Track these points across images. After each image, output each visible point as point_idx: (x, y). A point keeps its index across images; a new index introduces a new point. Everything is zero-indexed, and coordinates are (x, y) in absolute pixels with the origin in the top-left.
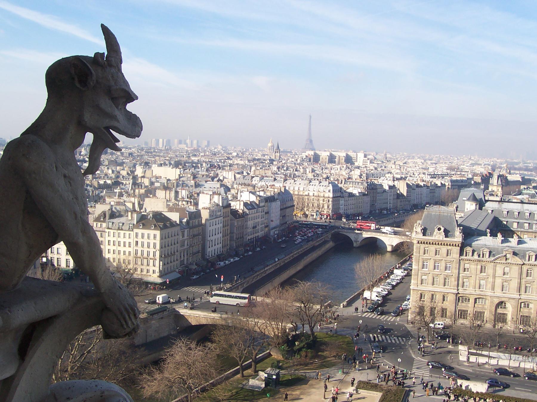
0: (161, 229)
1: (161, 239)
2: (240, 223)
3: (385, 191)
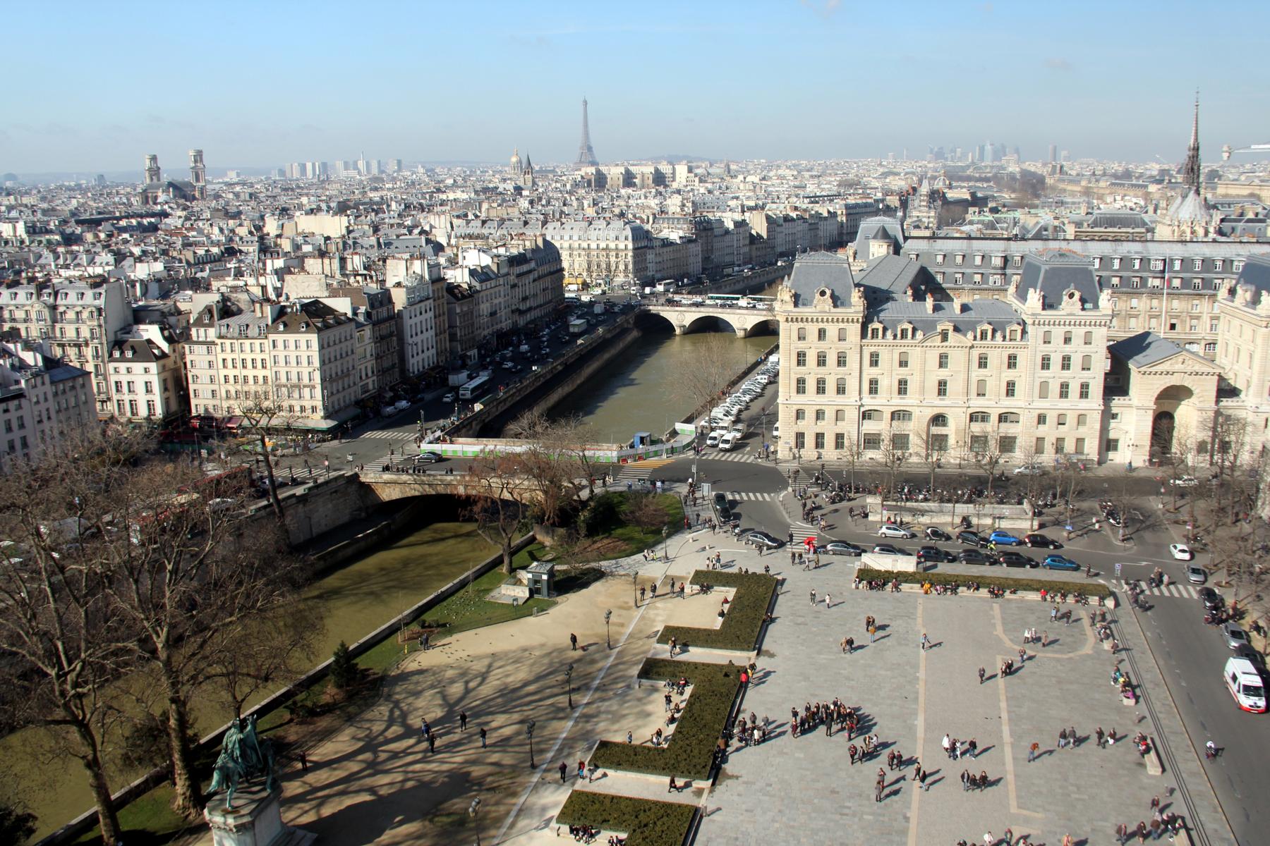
0: (319, 330)
1: (322, 347)
2: (465, 309)
3: (727, 232)
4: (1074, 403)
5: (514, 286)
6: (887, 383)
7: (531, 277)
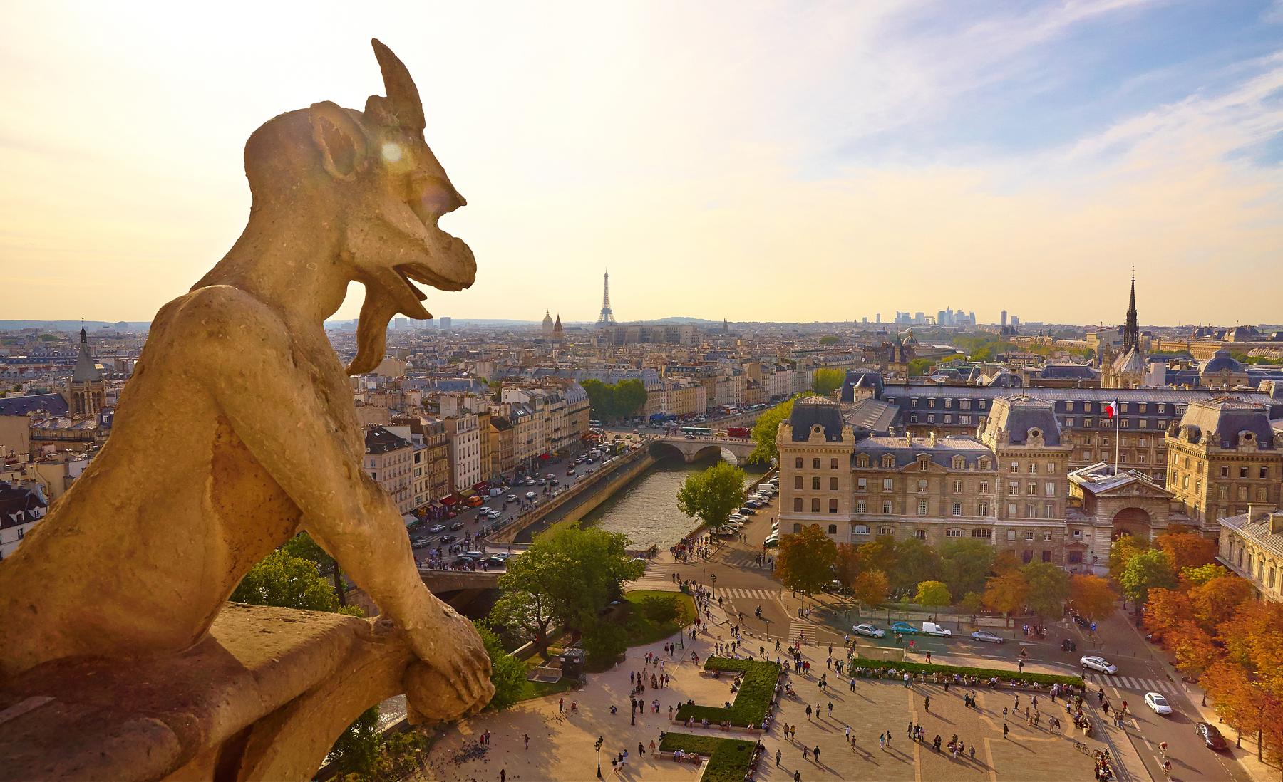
2: (506, 437)
5: (547, 420)
7: (562, 412)
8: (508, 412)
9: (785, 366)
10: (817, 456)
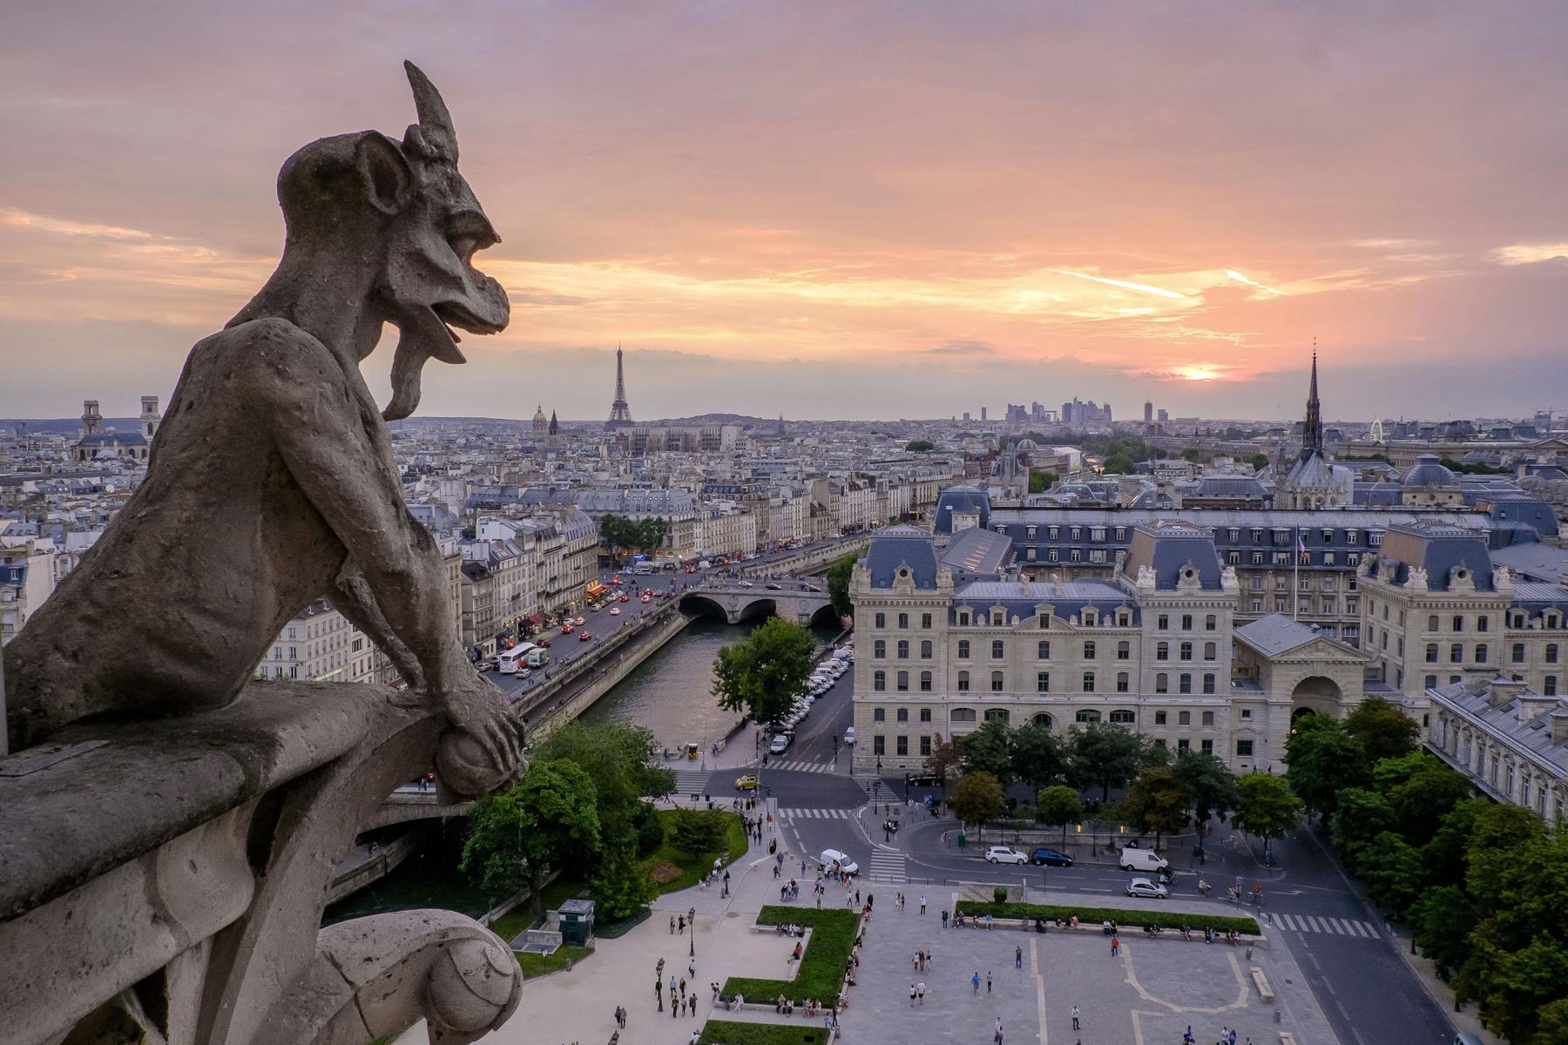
2: (483, 591)
4: (1198, 699)
5: (541, 565)
6: (980, 676)
8: (486, 556)
9: (860, 482)
10: (903, 610)
